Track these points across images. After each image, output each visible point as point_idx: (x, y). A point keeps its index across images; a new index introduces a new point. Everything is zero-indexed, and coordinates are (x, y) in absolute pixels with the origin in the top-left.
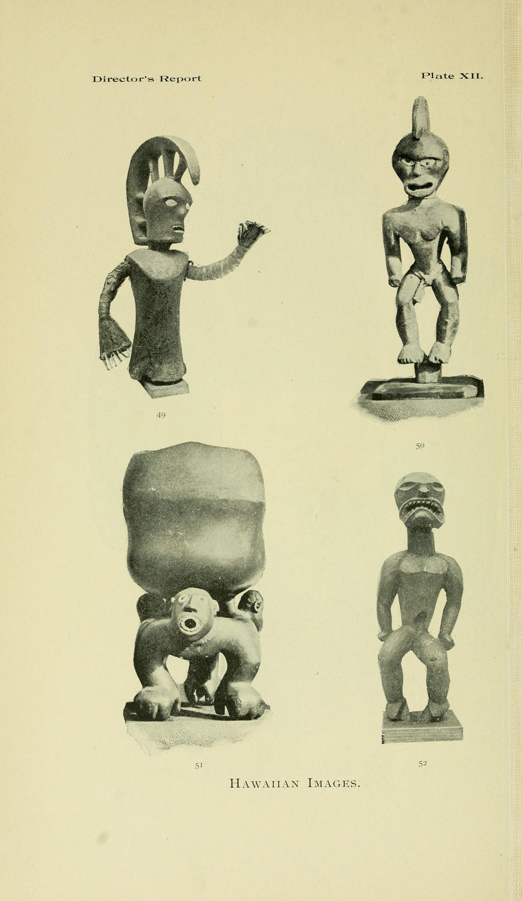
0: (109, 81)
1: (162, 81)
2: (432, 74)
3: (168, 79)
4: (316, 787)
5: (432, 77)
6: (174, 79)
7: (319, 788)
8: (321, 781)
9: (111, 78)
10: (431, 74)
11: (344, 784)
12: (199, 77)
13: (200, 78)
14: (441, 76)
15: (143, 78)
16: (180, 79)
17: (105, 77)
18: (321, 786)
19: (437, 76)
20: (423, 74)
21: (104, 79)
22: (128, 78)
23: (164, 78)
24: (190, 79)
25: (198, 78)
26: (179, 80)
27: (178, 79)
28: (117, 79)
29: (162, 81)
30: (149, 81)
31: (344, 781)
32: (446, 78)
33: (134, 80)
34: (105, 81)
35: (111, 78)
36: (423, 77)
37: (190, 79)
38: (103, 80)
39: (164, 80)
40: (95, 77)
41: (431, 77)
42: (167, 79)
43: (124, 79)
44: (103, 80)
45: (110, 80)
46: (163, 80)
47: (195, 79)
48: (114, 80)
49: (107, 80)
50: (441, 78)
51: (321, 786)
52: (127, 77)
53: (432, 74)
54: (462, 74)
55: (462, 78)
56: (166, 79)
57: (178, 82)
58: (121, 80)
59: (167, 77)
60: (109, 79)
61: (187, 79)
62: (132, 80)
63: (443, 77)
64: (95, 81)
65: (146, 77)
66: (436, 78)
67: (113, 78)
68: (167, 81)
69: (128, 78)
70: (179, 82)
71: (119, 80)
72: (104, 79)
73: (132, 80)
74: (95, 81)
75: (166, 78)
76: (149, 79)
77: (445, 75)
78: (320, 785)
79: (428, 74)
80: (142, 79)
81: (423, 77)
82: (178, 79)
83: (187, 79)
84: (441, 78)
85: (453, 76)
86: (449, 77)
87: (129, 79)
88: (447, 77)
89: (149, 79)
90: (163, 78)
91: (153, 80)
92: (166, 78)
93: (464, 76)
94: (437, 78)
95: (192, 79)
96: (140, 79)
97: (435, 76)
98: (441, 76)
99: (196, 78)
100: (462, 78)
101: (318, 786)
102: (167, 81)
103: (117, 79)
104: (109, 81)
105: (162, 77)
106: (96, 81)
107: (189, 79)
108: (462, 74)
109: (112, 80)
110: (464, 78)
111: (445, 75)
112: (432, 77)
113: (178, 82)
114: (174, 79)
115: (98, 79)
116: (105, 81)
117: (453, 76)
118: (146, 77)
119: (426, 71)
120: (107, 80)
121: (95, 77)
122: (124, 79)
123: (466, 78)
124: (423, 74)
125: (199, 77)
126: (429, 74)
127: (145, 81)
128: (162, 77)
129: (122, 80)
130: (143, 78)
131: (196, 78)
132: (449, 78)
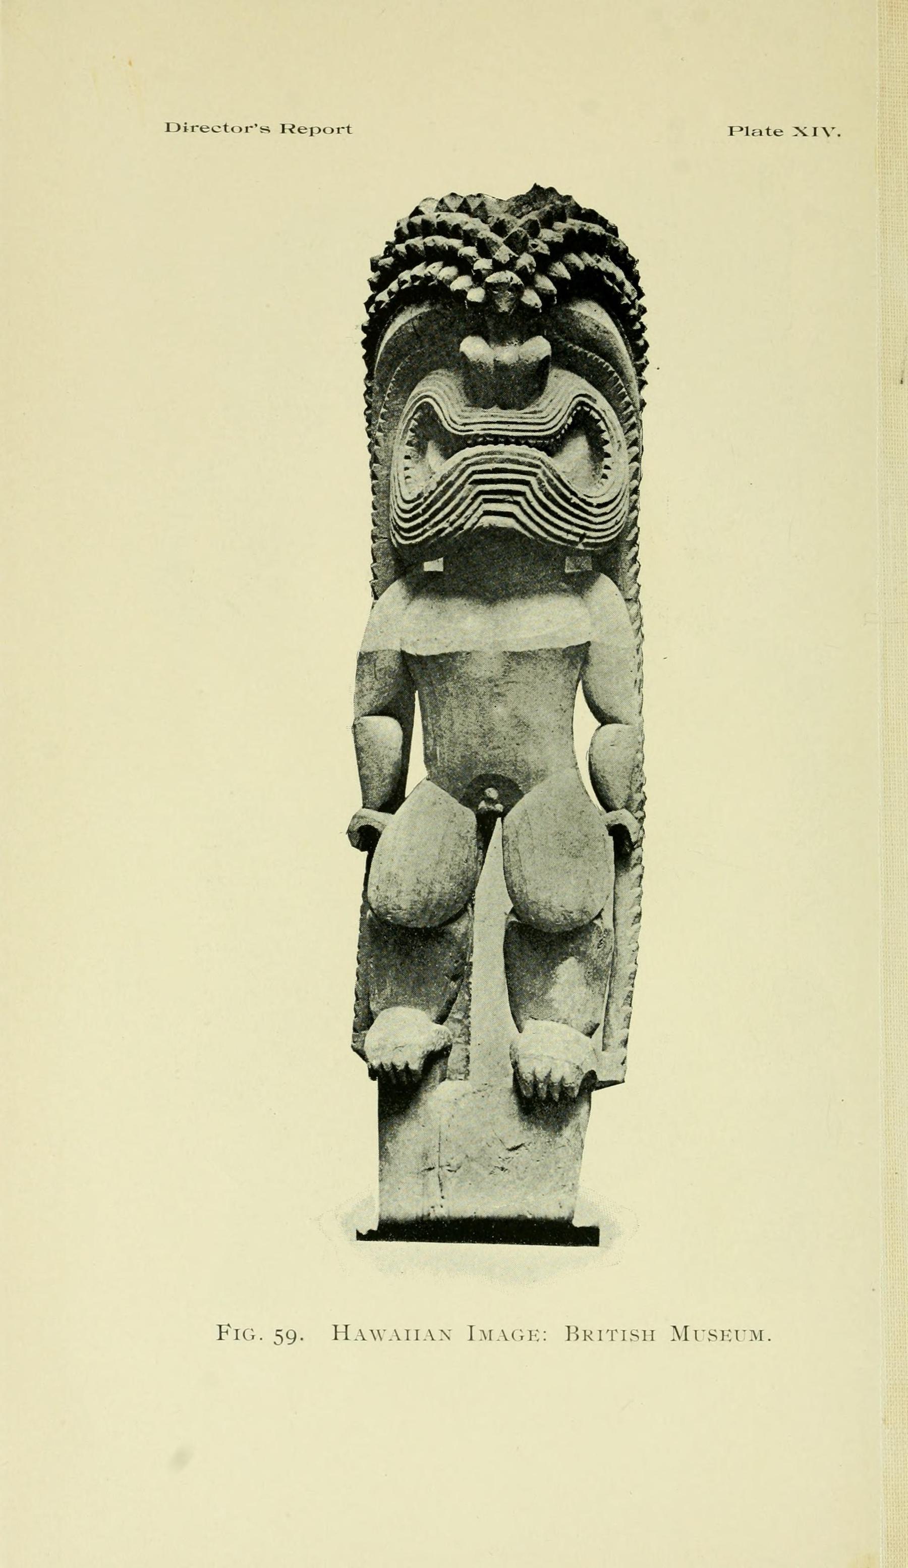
1: (283, 132)
2: (747, 128)
5: (747, 134)
6: (306, 129)
9: (197, 126)
10: (745, 129)
12: (348, 127)
13: (350, 129)
14: (761, 132)
15: (251, 127)
16: (316, 130)
17: (186, 124)
19: (754, 130)
20: (731, 128)
21: (185, 127)
22: (225, 126)
24: (333, 131)
26: (314, 131)
27: (312, 129)
28: (208, 128)
29: (283, 132)
30: (262, 132)
32: (770, 134)
33: (236, 129)
35: (197, 126)
36: (731, 134)
37: (333, 131)
39: (289, 131)
40: (168, 124)
41: (745, 134)
42: (293, 130)
43: (219, 127)
44: (182, 129)
46: (286, 131)
47: (341, 130)
48: (201, 129)
50: (761, 134)
52: (224, 124)
53: (747, 128)
56: (291, 130)
57: (312, 135)
58: (214, 129)
59: (294, 126)
61: (328, 131)
62: (232, 129)
63: (764, 132)
64: (168, 130)
65: (256, 125)
66: (753, 134)
67: (200, 127)
68: (292, 132)
69: (225, 126)
70: (313, 134)
71: (211, 129)
72: (185, 127)
73: (232, 129)
74: (168, 130)
75: (291, 127)
77: (768, 130)
79: (739, 129)
80: (249, 129)
81: (731, 134)
82: (312, 129)
83: (328, 131)
84: (761, 134)
85: (782, 131)
86: (775, 133)
87: (229, 129)
88: (771, 132)
90: (286, 127)
91: (269, 131)
92: (291, 127)
94: (755, 134)
95: (336, 131)
97: (750, 132)
98: (761, 132)
99: (343, 128)
102: (292, 132)
103: (208, 128)
105: (283, 126)
106: (170, 130)
109: (199, 128)
111: (768, 130)
112: (747, 134)
113: (312, 135)
114: (306, 129)
115: (173, 127)
116: (185, 130)
117: (782, 131)
118: (256, 125)
119: (736, 124)
121: (168, 124)
122: (219, 127)
123: (805, 135)
124: (731, 128)
125: (348, 127)
126: (742, 129)
128: (283, 126)
129: (216, 129)
130: (251, 127)
131: (343, 128)
132: (774, 135)
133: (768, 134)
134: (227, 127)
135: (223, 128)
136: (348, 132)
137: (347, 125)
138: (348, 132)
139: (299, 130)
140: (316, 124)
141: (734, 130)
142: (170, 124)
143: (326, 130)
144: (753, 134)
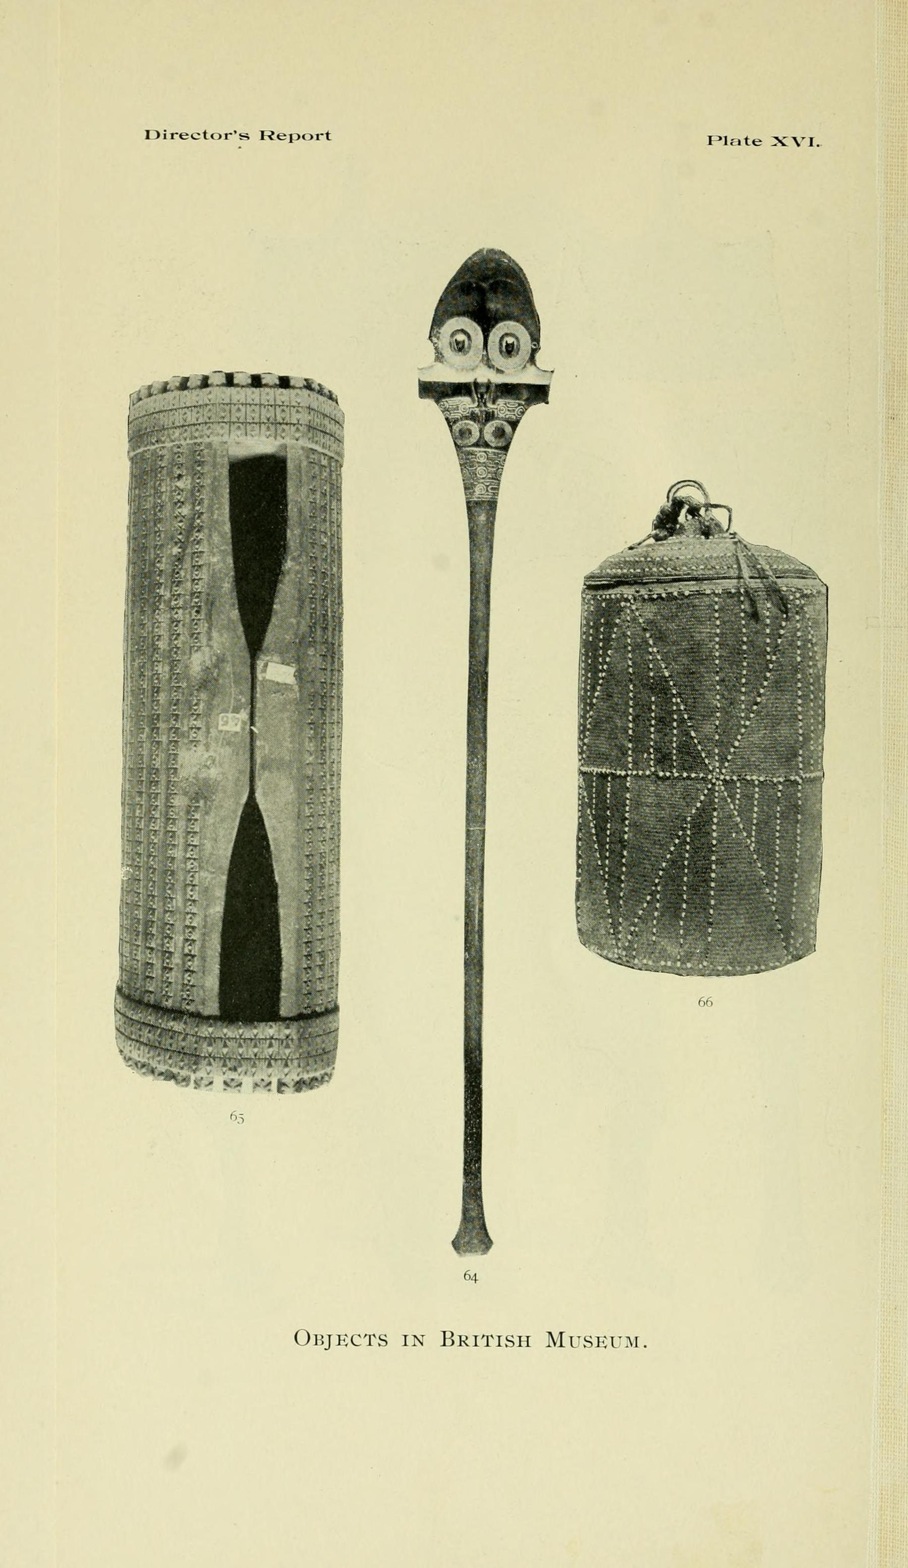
0: (172, 138)
1: (262, 138)
3: (274, 137)
4: (549, 1346)
5: (726, 144)
6: (285, 135)
7: (633, 1348)
8: (636, 1338)
9: (177, 133)
11: (599, 1342)
14: (739, 142)
15: (231, 134)
16: (295, 137)
17: (165, 131)
18: (636, 1346)
20: (710, 137)
21: (165, 135)
22: (205, 133)
23: (267, 133)
25: (325, 135)
27: (291, 135)
28: (187, 135)
29: (262, 138)
31: (598, 1338)
32: (749, 143)
33: (216, 136)
34: (165, 138)
35: (177, 133)
36: (710, 144)
37: (312, 137)
38: (162, 136)
40: (148, 132)
42: (272, 136)
43: (199, 134)
44: (162, 136)
45: (175, 136)
46: (265, 137)
47: (320, 136)
48: (181, 136)
49: (169, 136)
50: (739, 144)
51: (636, 1346)
53: (726, 137)
54: (777, 138)
55: (775, 145)
56: (270, 137)
57: (291, 142)
59: (273, 133)
60: (172, 135)
61: (308, 137)
63: (743, 142)
64: (148, 137)
65: (235, 132)
66: (731, 144)
68: (271, 139)
69: (205, 133)
72: (165, 135)
74: (148, 137)
75: (270, 133)
76: (240, 135)
77: (746, 139)
78: (634, 1345)
79: (718, 138)
80: (229, 136)
81: (710, 144)
82: (291, 135)
83: (308, 137)
84: (739, 144)
85: (760, 141)
86: (754, 142)
87: (208, 136)
88: (750, 142)
89: (240, 135)
90: (265, 134)
91: (248, 138)
92: (270, 134)
93: (780, 141)
95: (315, 137)
96: (226, 135)
97: (729, 142)
98: (739, 142)
99: (322, 134)
100: (775, 145)
101: (631, 1345)
102: (271, 139)
103: (187, 135)
104: (172, 138)
105: (263, 132)
106: (150, 137)
107: (310, 137)
108: (777, 138)
110: (780, 144)
111: (746, 139)
112: (726, 144)
113: (291, 142)
114: (285, 135)
115: (153, 135)
116: (165, 138)
117: (760, 141)
118: (235, 132)
120: (169, 136)
121: (148, 132)
122: (199, 134)
124: (710, 137)
125: (327, 134)
126: (721, 138)
127: (234, 138)
128: (263, 132)
129: (195, 136)
130: (231, 134)
131: (322, 134)
133: (746, 143)
134: (207, 135)
135: (202, 135)
136: (328, 138)
137: (325, 132)
138: (328, 138)
139: (278, 136)
140: (295, 131)
141: (713, 138)
142: (150, 132)
143: (306, 137)
144: (731, 144)
